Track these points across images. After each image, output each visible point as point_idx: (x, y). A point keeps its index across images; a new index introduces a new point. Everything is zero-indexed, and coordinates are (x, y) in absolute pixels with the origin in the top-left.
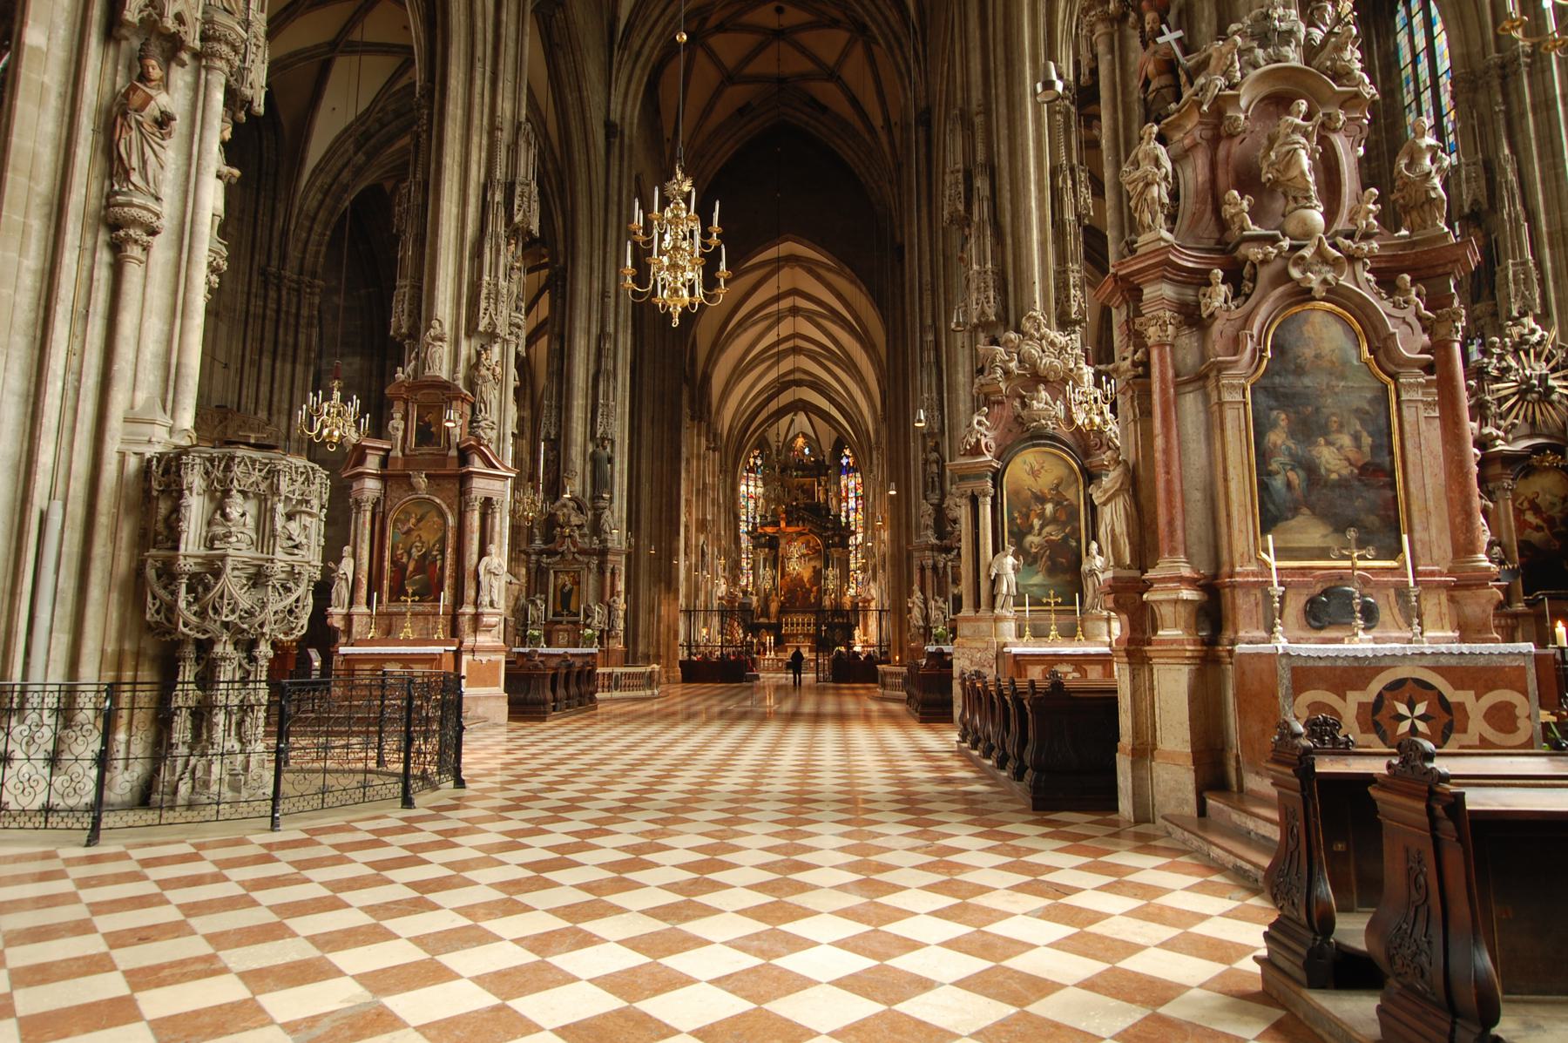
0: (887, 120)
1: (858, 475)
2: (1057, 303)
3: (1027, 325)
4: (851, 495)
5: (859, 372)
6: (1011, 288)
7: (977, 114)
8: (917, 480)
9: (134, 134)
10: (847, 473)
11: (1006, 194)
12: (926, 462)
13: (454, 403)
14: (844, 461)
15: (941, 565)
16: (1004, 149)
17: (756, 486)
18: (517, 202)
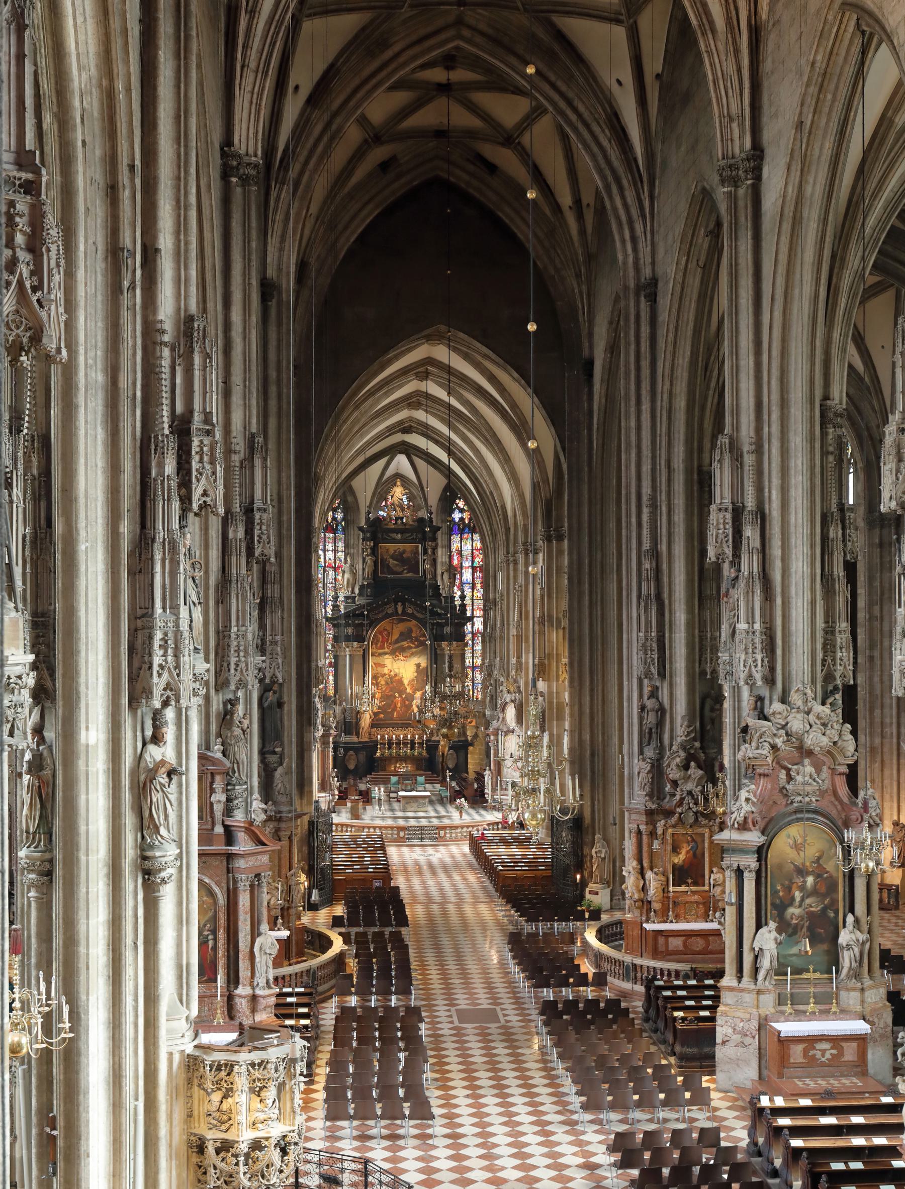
0: (577, 202)
1: (476, 537)
2: (823, 665)
3: (795, 698)
4: (467, 564)
5: (499, 442)
6: (779, 652)
7: (748, 452)
8: (630, 725)
9: (160, 794)
10: (462, 532)
11: (776, 551)
12: (643, 708)
13: (218, 778)
14: (457, 516)
15: (660, 831)
16: (775, 495)
17: (335, 551)
18: (257, 532)
